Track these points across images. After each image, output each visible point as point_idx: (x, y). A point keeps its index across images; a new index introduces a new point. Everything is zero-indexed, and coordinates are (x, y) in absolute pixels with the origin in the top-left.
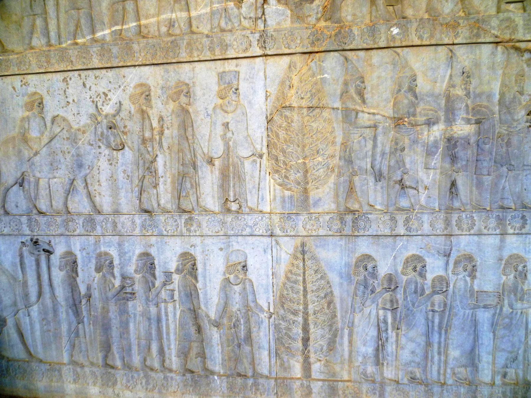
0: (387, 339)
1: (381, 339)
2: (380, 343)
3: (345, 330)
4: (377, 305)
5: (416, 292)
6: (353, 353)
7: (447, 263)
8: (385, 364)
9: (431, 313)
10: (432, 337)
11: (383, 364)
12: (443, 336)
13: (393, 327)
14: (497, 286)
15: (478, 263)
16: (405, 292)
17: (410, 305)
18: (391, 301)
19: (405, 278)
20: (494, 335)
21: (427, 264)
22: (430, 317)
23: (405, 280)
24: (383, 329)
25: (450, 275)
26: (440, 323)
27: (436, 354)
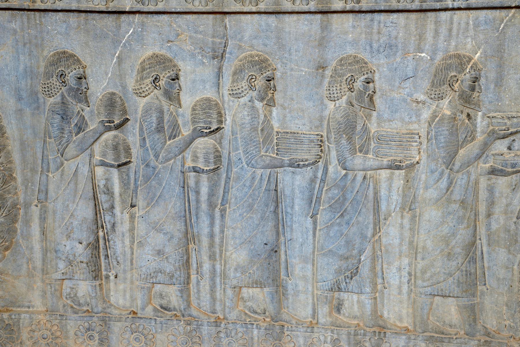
0: (114, 225)
1: (103, 227)
2: (101, 234)
3: (33, 207)
4: (91, 156)
5: (160, 129)
6: (49, 254)
7: (219, 74)
8: (112, 278)
9: (193, 174)
10: (197, 222)
11: (107, 277)
12: (217, 222)
13: (123, 202)
14: (317, 123)
15: (278, 74)
16: (141, 129)
17: (152, 157)
18: (115, 148)
19: (142, 102)
20: (315, 223)
21: (181, 73)
22: (192, 182)
23: (142, 105)
24: (106, 206)
25: (226, 98)
26: (212, 194)
27: (205, 258)
